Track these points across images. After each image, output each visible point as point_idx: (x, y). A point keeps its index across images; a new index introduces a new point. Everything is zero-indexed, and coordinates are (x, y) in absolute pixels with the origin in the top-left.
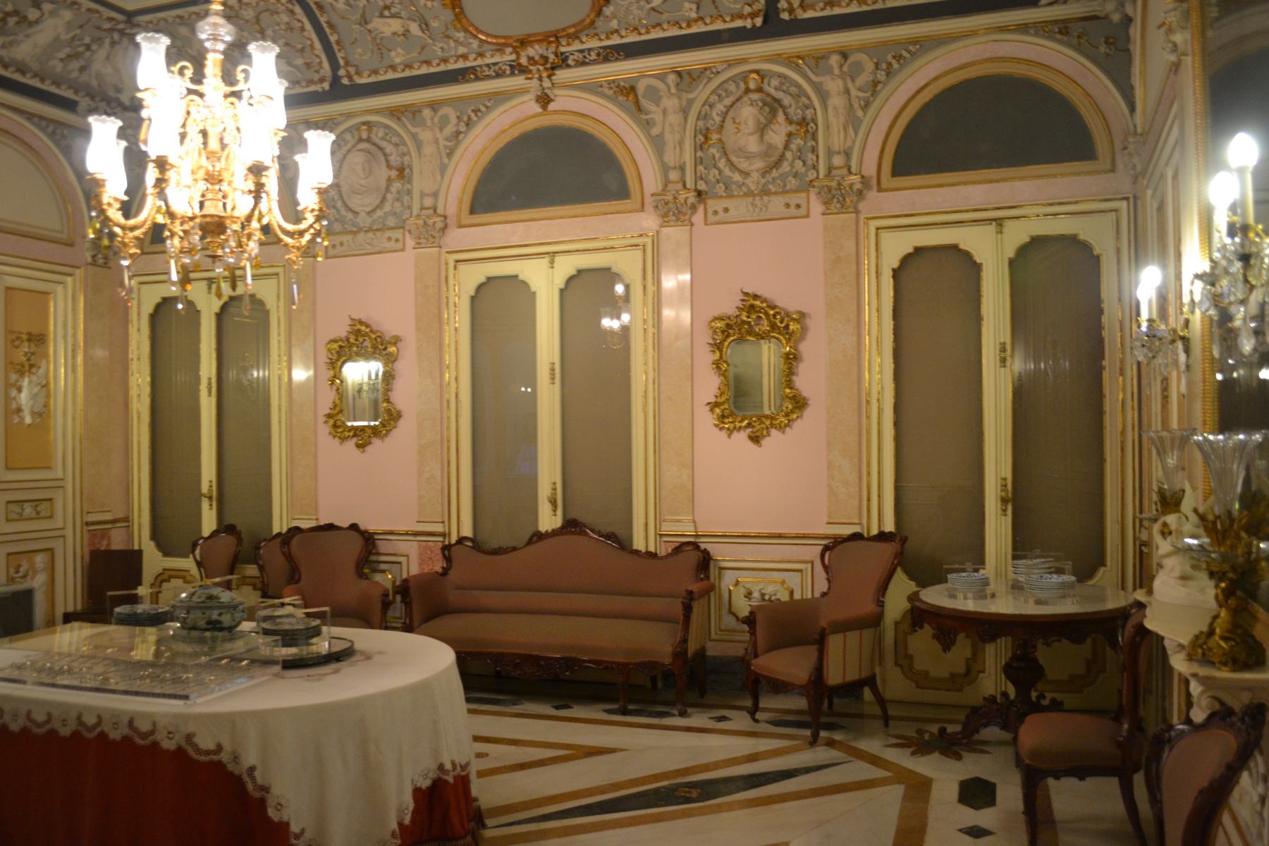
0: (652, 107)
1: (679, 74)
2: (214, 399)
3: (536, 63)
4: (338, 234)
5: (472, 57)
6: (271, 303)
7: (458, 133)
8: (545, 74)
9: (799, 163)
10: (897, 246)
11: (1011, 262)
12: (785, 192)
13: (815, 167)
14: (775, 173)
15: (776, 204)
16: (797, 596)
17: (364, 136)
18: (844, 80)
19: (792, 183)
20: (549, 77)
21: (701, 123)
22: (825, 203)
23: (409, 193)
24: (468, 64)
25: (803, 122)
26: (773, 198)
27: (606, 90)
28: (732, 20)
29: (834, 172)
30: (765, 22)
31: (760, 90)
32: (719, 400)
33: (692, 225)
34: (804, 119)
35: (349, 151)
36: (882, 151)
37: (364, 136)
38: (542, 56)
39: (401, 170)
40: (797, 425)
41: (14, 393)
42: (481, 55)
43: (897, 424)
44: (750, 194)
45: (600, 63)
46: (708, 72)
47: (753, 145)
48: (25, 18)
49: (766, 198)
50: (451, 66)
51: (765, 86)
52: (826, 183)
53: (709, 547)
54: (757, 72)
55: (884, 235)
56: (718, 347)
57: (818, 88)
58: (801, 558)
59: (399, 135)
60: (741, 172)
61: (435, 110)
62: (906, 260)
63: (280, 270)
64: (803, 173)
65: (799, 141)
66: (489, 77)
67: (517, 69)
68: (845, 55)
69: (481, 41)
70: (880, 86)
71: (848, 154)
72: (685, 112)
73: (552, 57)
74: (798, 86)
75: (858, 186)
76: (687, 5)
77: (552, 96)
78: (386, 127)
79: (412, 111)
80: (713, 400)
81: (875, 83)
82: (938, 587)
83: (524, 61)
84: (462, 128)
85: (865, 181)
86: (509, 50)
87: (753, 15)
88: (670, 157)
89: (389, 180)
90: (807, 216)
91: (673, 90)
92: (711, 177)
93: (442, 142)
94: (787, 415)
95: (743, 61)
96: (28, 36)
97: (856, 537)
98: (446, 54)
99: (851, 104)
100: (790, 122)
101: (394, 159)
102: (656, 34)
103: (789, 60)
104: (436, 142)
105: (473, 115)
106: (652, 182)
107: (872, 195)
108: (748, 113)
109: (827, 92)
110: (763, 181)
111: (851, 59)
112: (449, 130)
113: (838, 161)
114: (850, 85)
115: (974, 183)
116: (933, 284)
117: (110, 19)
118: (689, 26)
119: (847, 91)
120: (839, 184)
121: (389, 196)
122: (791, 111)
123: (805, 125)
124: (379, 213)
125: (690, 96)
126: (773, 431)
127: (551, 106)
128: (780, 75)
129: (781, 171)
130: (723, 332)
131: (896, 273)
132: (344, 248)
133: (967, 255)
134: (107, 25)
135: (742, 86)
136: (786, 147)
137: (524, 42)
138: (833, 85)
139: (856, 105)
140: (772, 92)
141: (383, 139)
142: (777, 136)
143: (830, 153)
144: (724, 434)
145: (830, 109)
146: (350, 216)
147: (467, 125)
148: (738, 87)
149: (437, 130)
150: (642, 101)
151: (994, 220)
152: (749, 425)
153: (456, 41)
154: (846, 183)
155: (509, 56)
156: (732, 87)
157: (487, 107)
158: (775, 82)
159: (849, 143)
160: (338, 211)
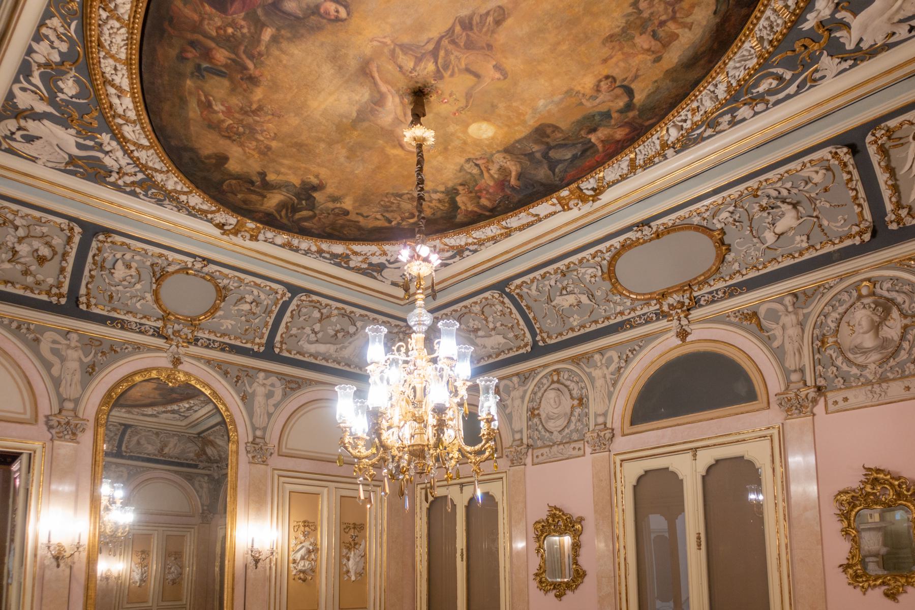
0: (774, 326)
1: (795, 295)
2: (465, 563)
3: (675, 308)
4: (540, 448)
5: (626, 312)
6: (498, 497)
7: (620, 368)
8: (682, 316)
12: (903, 377)
14: (892, 362)
15: (896, 389)
17: (555, 378)
20: (686, 317)
23: (587, 415)
24: (625, 318)
26: (892, 384)
27: (733, 319)
28: (841, 241)
31: (873, 294)
33: (814, 415)
35: (545, 391)
37: (555, 378)
38: (679, 302)
39: (581, 400)
41: (345, 561)
42: (634, 310)
44: (869, 383)
45: (726, 299)
46: (822, 289)
47: (869, 341)
48: (348, 332)
49: (884, 385)
50: (612, 322)
51: (878, 290)
54: (869, 280)
59: (579, 375)
60: (858, 366)
61: (602, 355)
63: (504, 475)
66: (641, 325)
67: (661, 315)
69: (632, 299)
72: (801, 325)
73: (687, 301)
76: (798, 238)
77: (689, 331)
78: (569, 370)
79: (587, 357)
83: (665, 308)
84: (623, 364)
86: (655, 302)
87: (861, 233)
88: (791, 362)
89: (573, 407)
91: (790, 309)
92: (829, 374)
93: (608, 377)
95: (856, 273)
96: (350, 343)
98: (608, 314)
101: (575, 393)
102: (771, 268)
104: (605, 377)
105: (630, 354)
106: (775, 384)
108: (862, 316)
110: (880, 370)
112: (613, 367)
117: (396, 326)
118: (801, 254)
121: (573, 418)
124: (567, 431)
125: (805, 311)
127: (689, 339)
129: (897, 360)
132: (545, 457)
134: (396, 330)
135: (855, 294)
136: (903, 338)
137: (664, 295)
140: (885, 294)
141: (567, 379)
142: (892, 329)
146: (548, 434)
147: (626, 361)
149: (604, 368)
150: (764, 323)
153: (615, 303)
155: (654, 307)
156: (845, 297)
157: (640, 347)
160: (540, 432)
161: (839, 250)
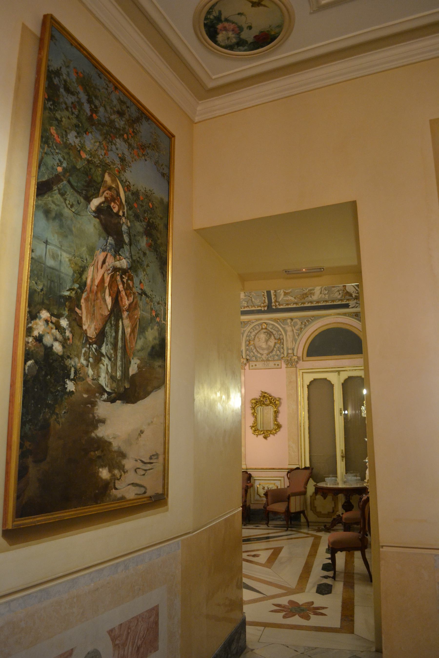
9: (278, 352)
10: (309, 378)
11: (343, 384)
12: (274, 360)
13: (283, 353)
14: (271, 354)
15: (271, 364)
16: (279, 487)
18: (292, 327)
19: (276, 358)
21: (247, 338)
22: (287, 365)
25: (279, 339)
26: (270, 362)
29: (289, 355)
30: (268, 309)
31: (266, 329)
32: (254, 425)
34: (280, 338)
36: (304, 349)
40: (278, 433)
43: (309, 433)
44: (263, 360)
47: (264, 346)
49: (268, 362)
51: (268, 328)
52: (287, 358)
53: (251, 473)
54: (265, 323)
55: (304, 375)
56: (253, 408)
57: (284, 329)
58: (280, 476)
60: (260, 354)
62: (311, 382)
64: (279, 355)
65: (278, 345)
68: (292, 319)
70: (303, 329)
71: (293, 350)
74: (278, 328)
75: (296, 360)
80: (252, 425)
81: (301, 328)
82: (323, 483)
85: (299, 358)
90: (281, 368)
94: (275, 430)
95: (261, 319)
97: (298, 469)
99: (294, 335)
100: (275, 339)
103: (276, 320)
107: (301, 362)
108: (263, 336)
109: (287, 330)
110: (267, 357)
111: (294, 321)
113: (290, 351)
114: (294, 328)
115: (331, 360)
116: (319, 390)
119: (293, 331)
120: (291, 359)
122: (276, 336)
123: (280, 340)
125: (244, 329)
126: (271, 435)
128: (272, 325)
130: (255, 404)
131: (308, 386)
133: (329, 382)
135: (261, 327)
136: (274, 347)
138: (289, 329)
139: (296, 335)
140: (270, 329)
142: (272, 343)
143: (288, 349)
144: (255, 436)
145: (288, 336)
148: (259, 327)
151: (337, 371)
152: (263, 433)
154: (293, 359)
156: (257, 327)
158: (271, 326)
159: (294, 346)
161: (257, 310)
